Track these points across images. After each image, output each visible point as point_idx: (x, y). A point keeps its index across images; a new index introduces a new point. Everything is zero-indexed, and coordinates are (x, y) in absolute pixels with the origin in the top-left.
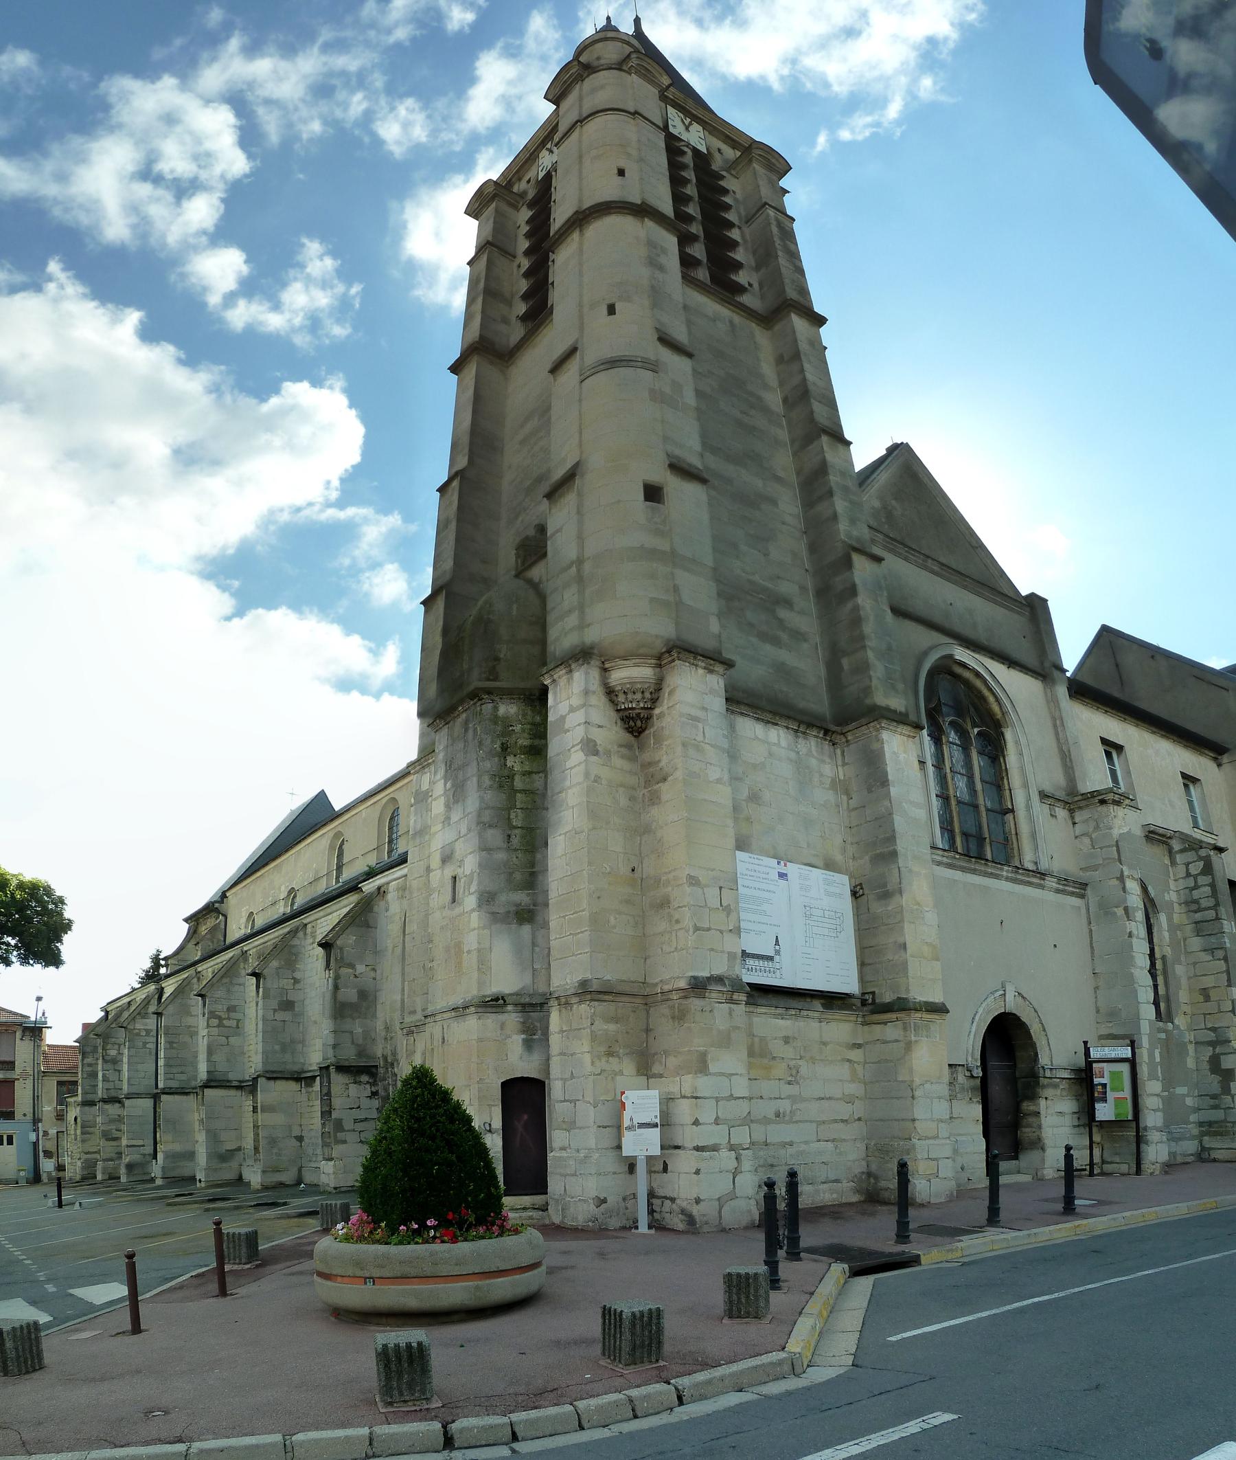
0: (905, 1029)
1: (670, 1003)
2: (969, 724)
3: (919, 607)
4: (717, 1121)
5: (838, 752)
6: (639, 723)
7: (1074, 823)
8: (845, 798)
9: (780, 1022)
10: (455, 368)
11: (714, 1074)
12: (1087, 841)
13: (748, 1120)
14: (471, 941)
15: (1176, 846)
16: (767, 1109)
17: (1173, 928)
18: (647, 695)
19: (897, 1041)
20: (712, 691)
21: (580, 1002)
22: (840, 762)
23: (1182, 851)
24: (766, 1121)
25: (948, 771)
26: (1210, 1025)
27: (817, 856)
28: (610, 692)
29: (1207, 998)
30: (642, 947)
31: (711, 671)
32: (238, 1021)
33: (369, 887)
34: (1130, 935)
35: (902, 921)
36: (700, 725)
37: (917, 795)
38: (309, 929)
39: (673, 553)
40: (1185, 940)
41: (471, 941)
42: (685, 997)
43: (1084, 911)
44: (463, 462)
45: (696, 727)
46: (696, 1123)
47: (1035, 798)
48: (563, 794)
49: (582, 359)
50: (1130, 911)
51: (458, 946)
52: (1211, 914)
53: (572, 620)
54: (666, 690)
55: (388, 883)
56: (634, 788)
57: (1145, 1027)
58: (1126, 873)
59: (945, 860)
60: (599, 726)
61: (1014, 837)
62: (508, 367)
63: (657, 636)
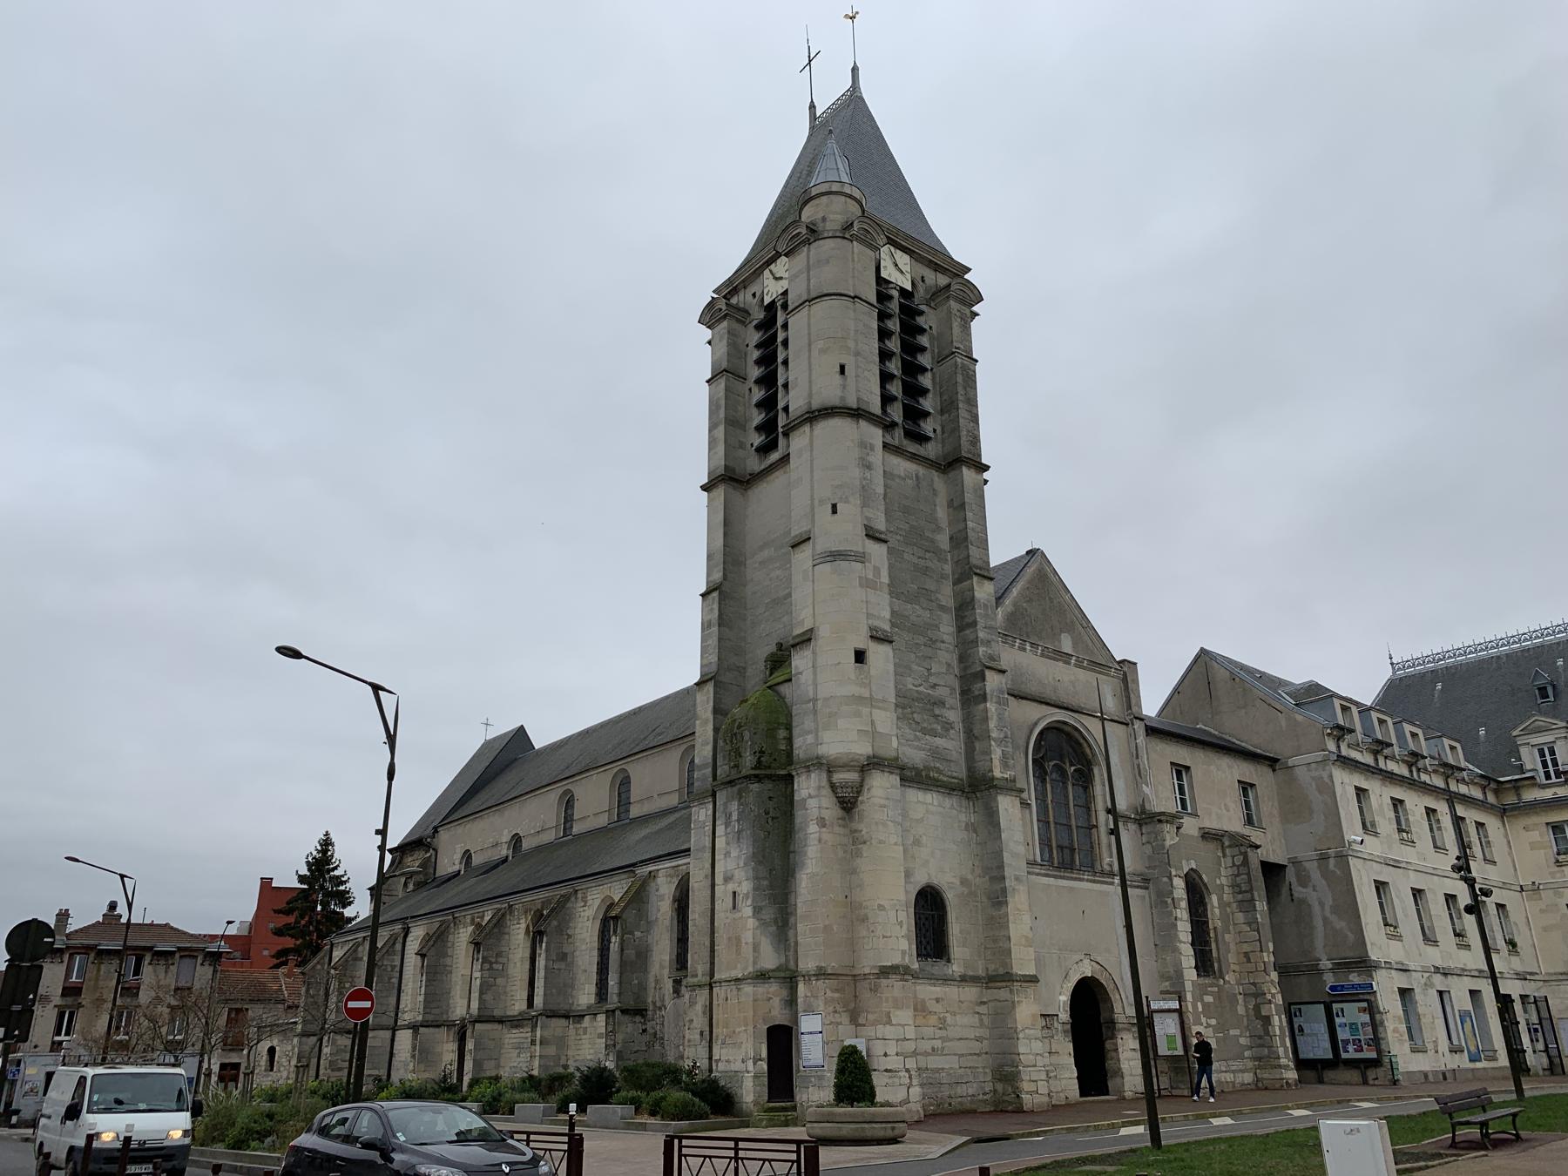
0: (1011, 991)
2: (1068, 764)
3: (1033, 689)
4: (897, 1054)
5: (971, 804)
7: (1142, 834)
8: (975, 835)
10: (705, 488)
12: (1149, 846)
13: (915, 1054)
14: (748, 937)
16: (926, 1046)
17: (1222, 905)
18: (855, 789)
19: (1007, 1001)
21: (817, 980)
22: (972, 811)
24: (926, 1054)
28: (833, 786)
29: (1249, 961)
30: (852, 944)
33: (643, 871)
35: (1008, 922)
37: (1019, 837)
38: (580, 895)
41: (748, 937)
42: (878, 978)
44: (718, 576)
46: (886, 1055)
48: (806, 848)
49: (814, 546)
50: (1176, 901)
51: (738, 939)
53: (810, 739)
54: (866, 787)
55: (658, 870)
56: (846, 845)
57: (1188, 986)
58: (1174, 873)
59: (1043, 872)
60: (827, 809)
61: (1097, 846)
63: (861, 755)
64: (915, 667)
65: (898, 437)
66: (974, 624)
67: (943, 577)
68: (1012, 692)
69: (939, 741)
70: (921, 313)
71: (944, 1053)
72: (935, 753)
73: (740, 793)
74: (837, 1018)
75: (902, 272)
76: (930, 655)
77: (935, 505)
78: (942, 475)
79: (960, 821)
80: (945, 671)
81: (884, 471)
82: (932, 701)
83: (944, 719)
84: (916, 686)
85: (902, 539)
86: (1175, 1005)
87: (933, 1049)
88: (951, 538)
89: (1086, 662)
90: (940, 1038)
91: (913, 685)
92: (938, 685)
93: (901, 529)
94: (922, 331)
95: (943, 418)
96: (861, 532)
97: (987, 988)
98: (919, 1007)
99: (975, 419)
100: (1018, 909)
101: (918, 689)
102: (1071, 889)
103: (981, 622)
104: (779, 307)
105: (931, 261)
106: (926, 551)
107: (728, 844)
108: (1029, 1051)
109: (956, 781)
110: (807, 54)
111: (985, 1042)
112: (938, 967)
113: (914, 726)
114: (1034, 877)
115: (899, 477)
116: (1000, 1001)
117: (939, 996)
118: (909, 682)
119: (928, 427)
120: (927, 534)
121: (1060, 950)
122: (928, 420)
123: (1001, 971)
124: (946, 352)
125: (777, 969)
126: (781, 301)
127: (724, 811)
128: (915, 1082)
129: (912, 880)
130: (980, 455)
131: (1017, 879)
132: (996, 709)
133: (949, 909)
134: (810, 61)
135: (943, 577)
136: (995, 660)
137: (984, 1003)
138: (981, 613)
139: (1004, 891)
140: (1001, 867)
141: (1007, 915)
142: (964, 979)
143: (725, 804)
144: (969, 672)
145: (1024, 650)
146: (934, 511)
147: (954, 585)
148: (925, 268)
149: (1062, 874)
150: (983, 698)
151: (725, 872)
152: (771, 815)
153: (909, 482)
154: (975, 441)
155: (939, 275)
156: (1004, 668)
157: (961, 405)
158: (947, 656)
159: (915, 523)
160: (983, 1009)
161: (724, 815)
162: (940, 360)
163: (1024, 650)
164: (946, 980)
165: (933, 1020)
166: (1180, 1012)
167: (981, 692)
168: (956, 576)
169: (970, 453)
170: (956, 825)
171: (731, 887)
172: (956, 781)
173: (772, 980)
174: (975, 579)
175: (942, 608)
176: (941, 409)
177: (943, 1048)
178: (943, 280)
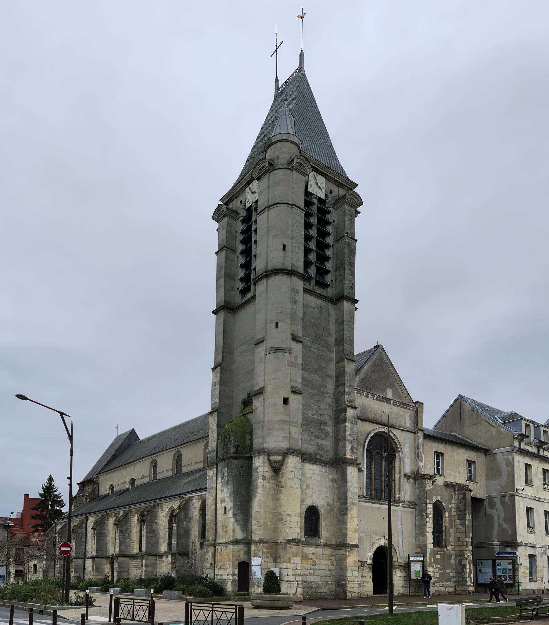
1: (282, 545)
5: (335, 470)
6: (277, 470)
8: (335, 484)
9: (311, 549)
11: (292, 563)
14: (231, 526)
15: (456, 489)
20: (297, 462)
21: (260, 544)
22: (335, 473)
23: (458, 490)
25: (373, 469)
26: (459, 549)
30: (276, 530)
31: (297, 456)
32: (129, 534)
34: (426, 522)
35: (347, 522)
36: (294, 473)
37: (356, 485)
39: (290, 421)
40: (455, 520)
41: (231, 526)
42: (286, 544)
43: (414, 513)
45: (292, 474)
47: (402, 476)
51: (226, 526)
52: (463, 513)
59: (366, 500)
62: (235, 313)
64: (313, 406)
65: (312, 285)
66: (343, 384)
67: (330, 360)
68: (358, 418)
70: (329, 212)
71: (314, 575)
72: (320, 447)
73: (228, 464)
74: (268, 560)
76: (321, 400)
77: (329, 322)
78: (334, 306)
81: (304, 304)
82: (320, 422)
83: (325, 431)
84: (313, 415)
85: (311, 340)
87: (309, 573)
88: (336, 340)
90: (312, 569)
91: (312, 415)
92: (324, 415)
94: (329, 223)
95: (337, 273)
96: (289, 337)
97: (335, 549)
98: (304, 556)
99: (353, 274)
100: (352, 517)
101: (313, 416)
103: (347, 383)
104: (254, 210)
105: (336, 181)
106: (323, 346)
107: (222, 486)
108: (352, 575)
109: (328, 460)
110: (275, 44)
111: (333, 571)
113: (310, 434)
114: (362, 503)
115: (312, 307)
116: (340, 555)
117: (314, 552)
118: (310, 414)
119: (328, 279)
120: (324, 338)
121: (371, 534)
122: (329, 275)
123: (342, 542)
124: (340, 236)
125: (243, 539)
126: (255, 206)
127: (221, 472)
128: (300, 586)
129: (304, 504)
130: (354, 295)
131: (353, 504)
132: (350, 426)
133: (321, 516)
134: (277, 49)
135: (330, 360)
136: (352, 402)
137: (334, 556)
138: (347, 379)
139: (346, 509)
140: (346, 498)
141: (347, 519)
142: (325, 546)
143: (222, 469)
144: (339, 408)
146: (328, 325)
147: (336, 364)
148: (333, 185)
150: (345, 421)
151: (221, 499)
152: (242, 474)
153: (316, 310)
154: (352, 286)
155: (340, 189)
156: (356, 406)
157: (346, 266)
158: (329, 400)
159: (318, 332)
160: (333, 558)
161: (221, 474)
162: (337, 240)
164: (317, 546)
165: (310, 562)
166: (423, 562)
167: (344, 418)
168: (337, 360)
169: (349, 293)
170: (327, 480)
171: (224, 505)
172: (328, 460)
173: (241, 544)
174: (346, 361)
175: (329, 376)
176: (336, 269)
177: (314, 573)
178: (342, 192)
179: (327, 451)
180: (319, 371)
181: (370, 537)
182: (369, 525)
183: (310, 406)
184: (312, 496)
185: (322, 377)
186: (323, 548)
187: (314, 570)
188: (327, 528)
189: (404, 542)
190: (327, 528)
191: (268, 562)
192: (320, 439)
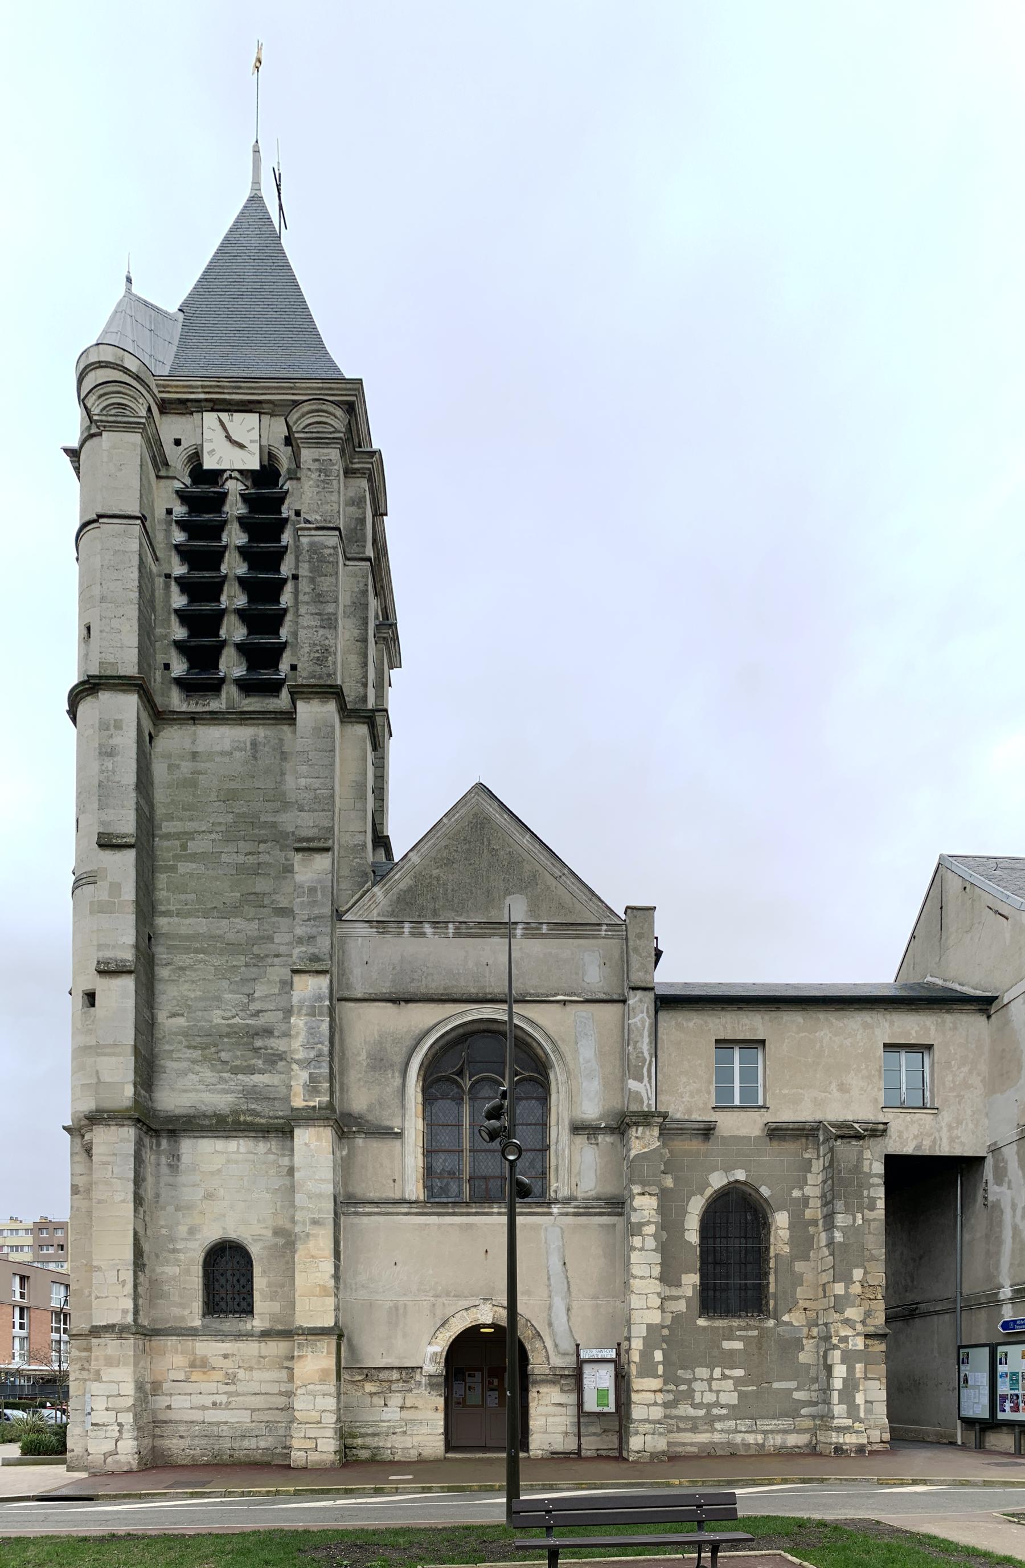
27: (267, 1228)
60: (81, 1175)
64: (228, 996)
69: (258, 1079)
71: (230, 1407)
72: (252, 1093)
75: (241, 446)
76: (253, 976)
79: (280, 1166)
80: (277, 991)
85: (219, 837)
86: (612, 1354)
87: (214, 1404)
89: (544, 927)
90: (225, 1393)
91: (224, 1018)
92: (265, 1011)
93: (220, 824)
98: (198, 1363)
101: (230, 1022)
102: (470, 1226)
106: (260, 842)
109: (282, 1121)
112: (230, 1324)
113: (220, 1067)
115: (222, 753)
121: (437, 1296)
129: (197, 1237)
142: (266, 1334)
145: (423, 935)
149: (450, 1210)
153: (237, 754)
163: (423, 935)
165: (218, 1375)
170: (272, 1172)
172: (282, 1121)
179: (274, 1099)
180: (246, 907)
181: (434, 1305)
182: (431, 1272)
183: (219, 999)
184: (224, 1216)
185: (259, 919)
186: (260, 1342)
187: (229, 1394)
188: (276, 1292)
189: (574, 1312)
190: (276, 1292)
191: (86, 1380)
192: (253, 1074)
